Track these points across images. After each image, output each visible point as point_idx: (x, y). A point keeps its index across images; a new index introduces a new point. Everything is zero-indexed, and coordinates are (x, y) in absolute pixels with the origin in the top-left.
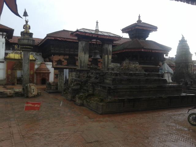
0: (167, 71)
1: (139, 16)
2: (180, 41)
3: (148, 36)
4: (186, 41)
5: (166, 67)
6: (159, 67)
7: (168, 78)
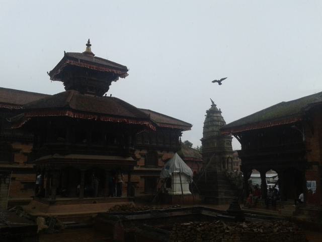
0: (178, 171)
1: (89, 42)
2: (207, 112)
3: (107, 89)
4: (220, 112)
5: (178, 162)
6: (131, 159)
7: (181, 188)
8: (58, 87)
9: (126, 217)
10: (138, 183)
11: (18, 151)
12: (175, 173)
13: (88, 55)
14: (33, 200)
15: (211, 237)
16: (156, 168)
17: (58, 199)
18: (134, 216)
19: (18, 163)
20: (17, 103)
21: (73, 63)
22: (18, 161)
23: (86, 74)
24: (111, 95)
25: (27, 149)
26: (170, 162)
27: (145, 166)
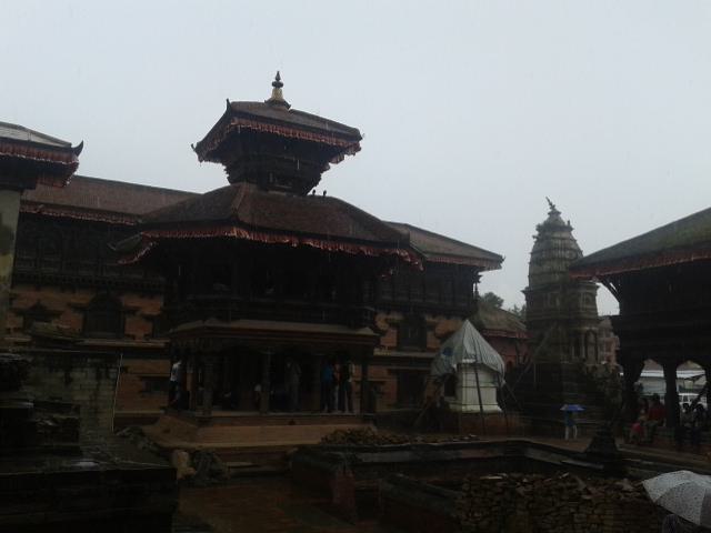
0: (471, 361)
1: (278, 78)
2: (539, 228)
4: (569, 228)
5: (471, 341)
6: (367, 331)
7: (479, 398)
8: (212, 178)
9: (359, 457)
10: (382, 383)
11: (133, 311)
12: (465, 364)
13: (276, 106)
14: (166, 413)
15: (550, 510)
16: (423, 351)
17: (215, 413)
18: (376, 455)
19: (134, 337)
20: (130, 211)
21: (246, 124)
22: (131, 333)
23: (273, 146)
24: (325, 193)
25: (153, 306)
26: (455, 339)
27: (398, 348)
